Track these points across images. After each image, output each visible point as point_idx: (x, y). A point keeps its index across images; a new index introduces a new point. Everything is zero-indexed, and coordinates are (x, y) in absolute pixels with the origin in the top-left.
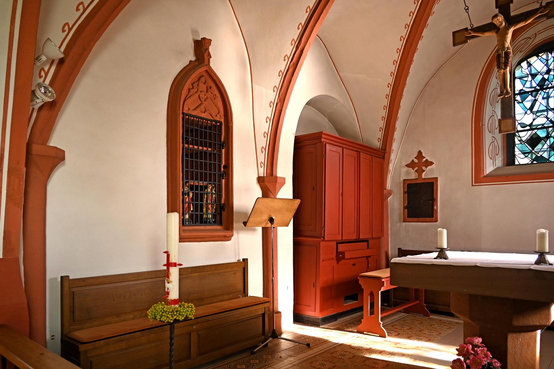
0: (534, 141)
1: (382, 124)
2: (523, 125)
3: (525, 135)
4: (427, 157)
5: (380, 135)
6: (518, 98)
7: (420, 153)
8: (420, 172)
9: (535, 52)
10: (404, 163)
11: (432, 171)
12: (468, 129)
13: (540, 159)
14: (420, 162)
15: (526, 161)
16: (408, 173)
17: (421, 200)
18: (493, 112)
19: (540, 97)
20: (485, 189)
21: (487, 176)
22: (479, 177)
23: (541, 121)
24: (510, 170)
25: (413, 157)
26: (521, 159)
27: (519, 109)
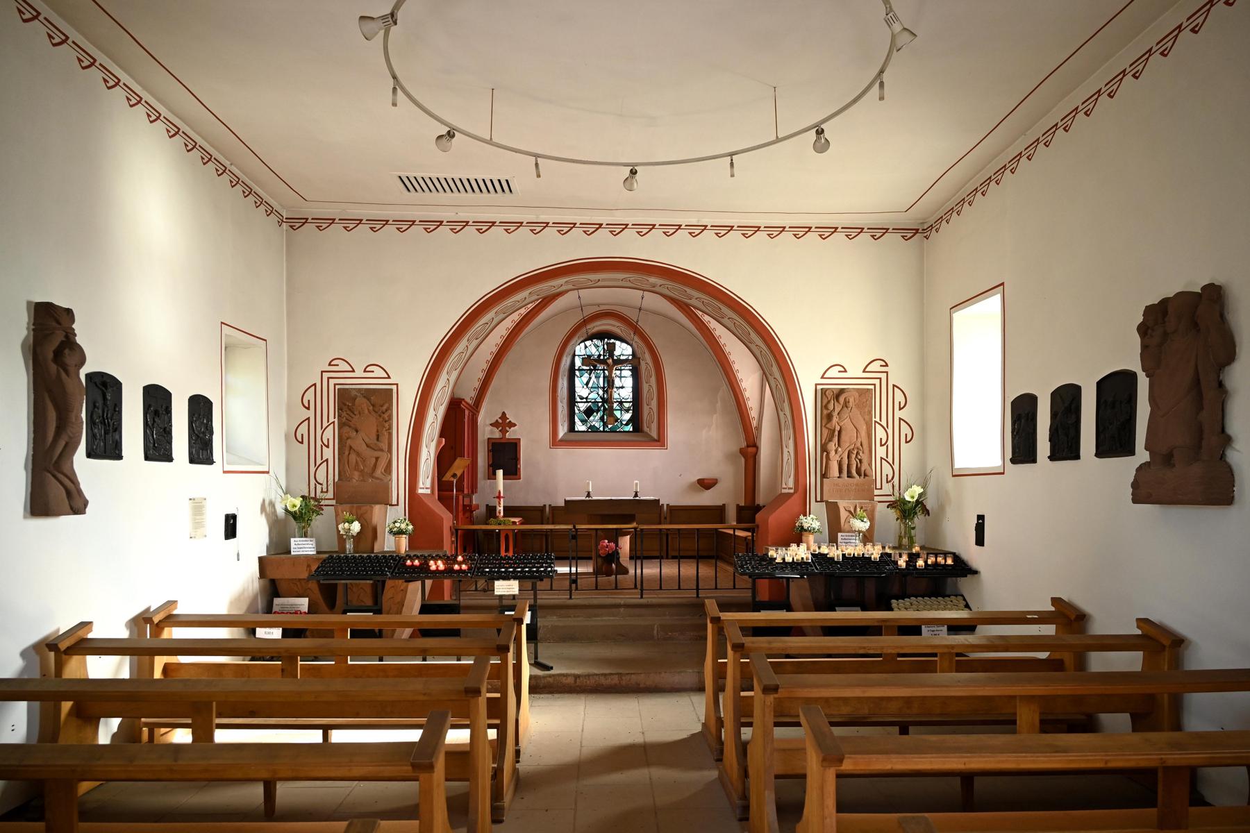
0: (589, 412)
1: (477, 385)
2: (582, 398)
3: (583, 406)
4: (511, 418)
5: (473, 394)
6: (577, 373)
7: (504, 413)
8: (504, 432)
9: (591, 338)
10: (489, 422)
11: (515, 432)
12: (546, 397)
13: (593, 429)
14: (503, 423)
15: (583, 428)
16: (492, 432)
17: (506, 456)
18: (563, 383)
19: (593, 376)
20: (560, 452)
21: (561, 441)
22: (555, 442)
23: (593, 396)
24: (573, 436)
25: (497, 417)
26: (580, 427)
27: (577, 382)
